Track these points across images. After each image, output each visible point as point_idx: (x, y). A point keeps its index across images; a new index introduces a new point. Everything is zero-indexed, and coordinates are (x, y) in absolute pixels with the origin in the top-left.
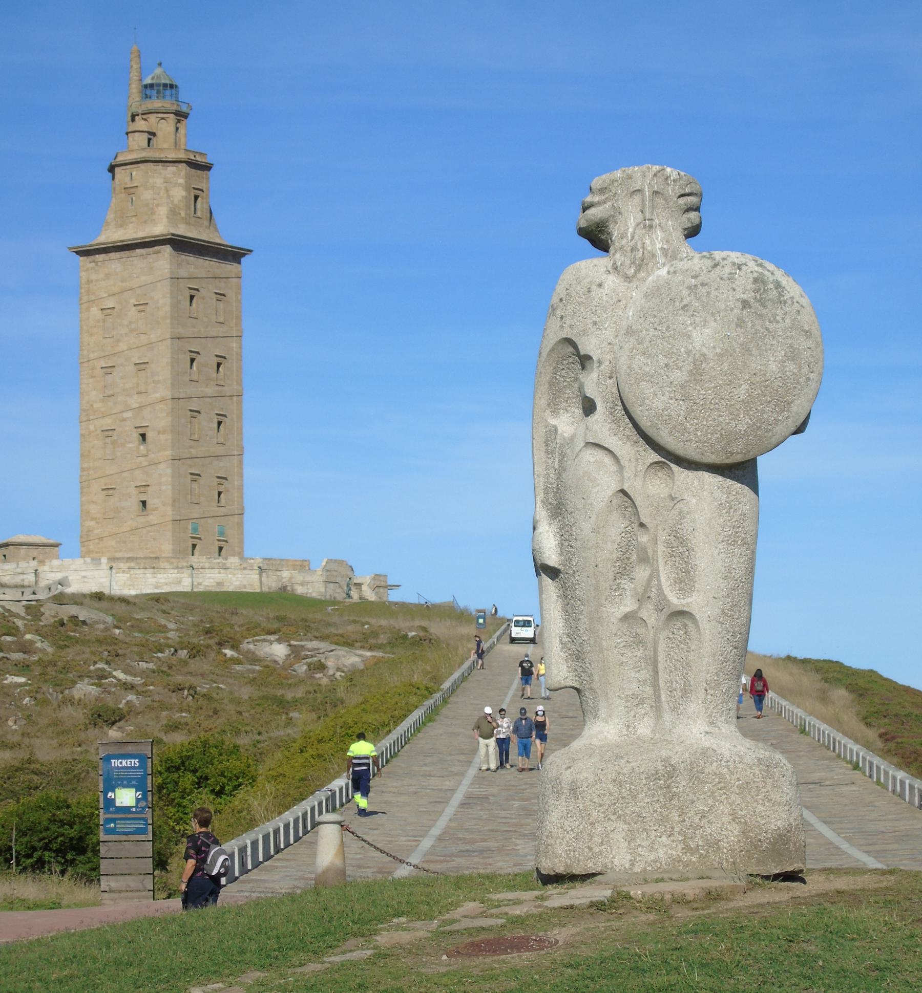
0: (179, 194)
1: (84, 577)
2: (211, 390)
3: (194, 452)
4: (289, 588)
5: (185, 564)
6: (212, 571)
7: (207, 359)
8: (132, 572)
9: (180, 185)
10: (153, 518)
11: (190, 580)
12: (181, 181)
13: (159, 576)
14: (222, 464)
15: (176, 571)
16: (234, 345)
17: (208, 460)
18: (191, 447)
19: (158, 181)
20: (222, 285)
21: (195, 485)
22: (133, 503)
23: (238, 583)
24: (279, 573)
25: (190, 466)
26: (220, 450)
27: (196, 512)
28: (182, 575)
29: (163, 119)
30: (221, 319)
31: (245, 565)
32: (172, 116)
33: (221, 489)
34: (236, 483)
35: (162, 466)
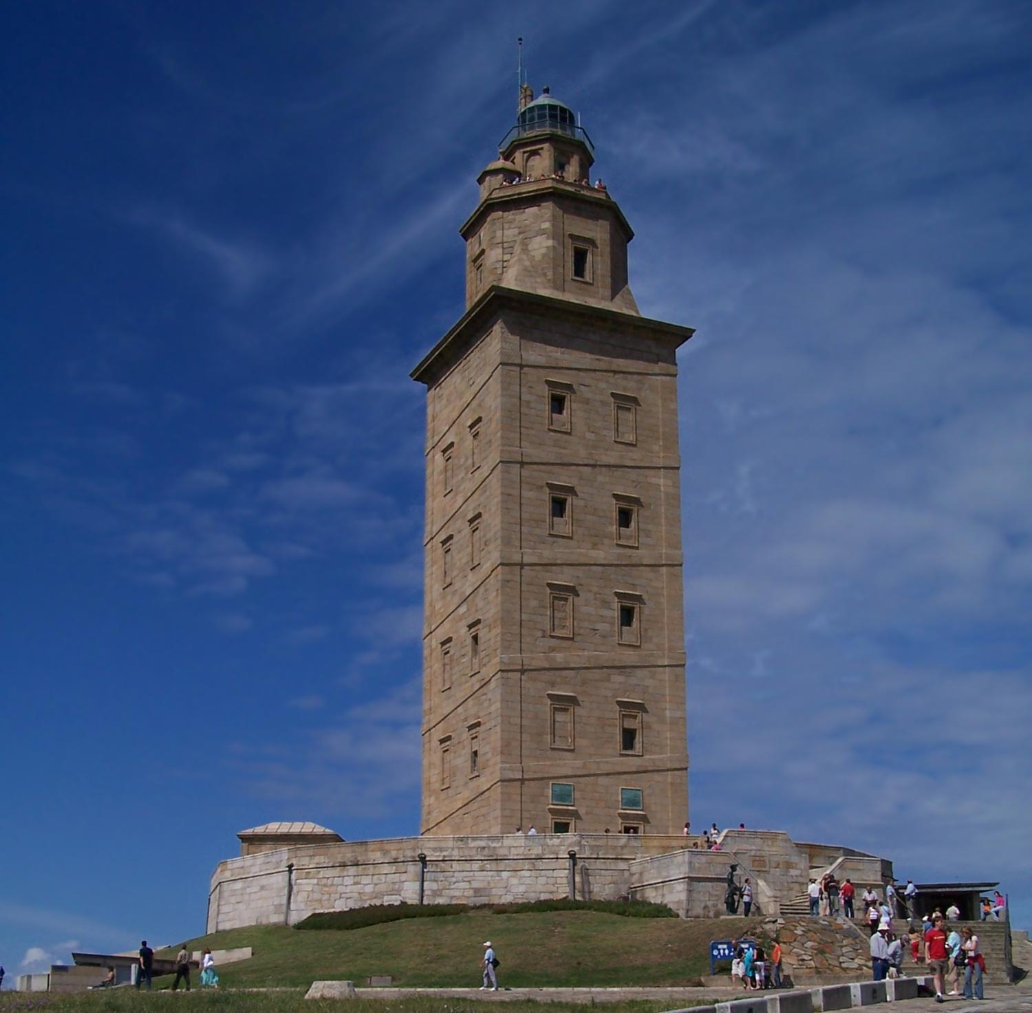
0: (541, 246)
1: (262, 888)
2: (600, 555)
3: (559, 657)
4: (638, 896)
5: (409, 853)
6: (467, 866)
7: (596, 498)
8: (323, 873)
9: (542, 232)
10: (483, 783)
11: (417, 885)
12: (546, 225)
13: (365, 880)
14: (633, 681)
15: (393, 868)
16: (662, 481)
17: (597, 674)
18: (552, 649)
19: (510, 233)
20: (632, 384)
21: (560, 717)
22: (461, 759)
23: (522, 889)
24: (622, 865)
25: (553, 685)
26: (630, 657)
27: (567, 765)
28: (404, 877)
29: (535, 153)
30: (631, 438)
31: (536, 851)
32: (546, 146)
33: (629, 724)
34: (668, 713)
35: (493, 684)
